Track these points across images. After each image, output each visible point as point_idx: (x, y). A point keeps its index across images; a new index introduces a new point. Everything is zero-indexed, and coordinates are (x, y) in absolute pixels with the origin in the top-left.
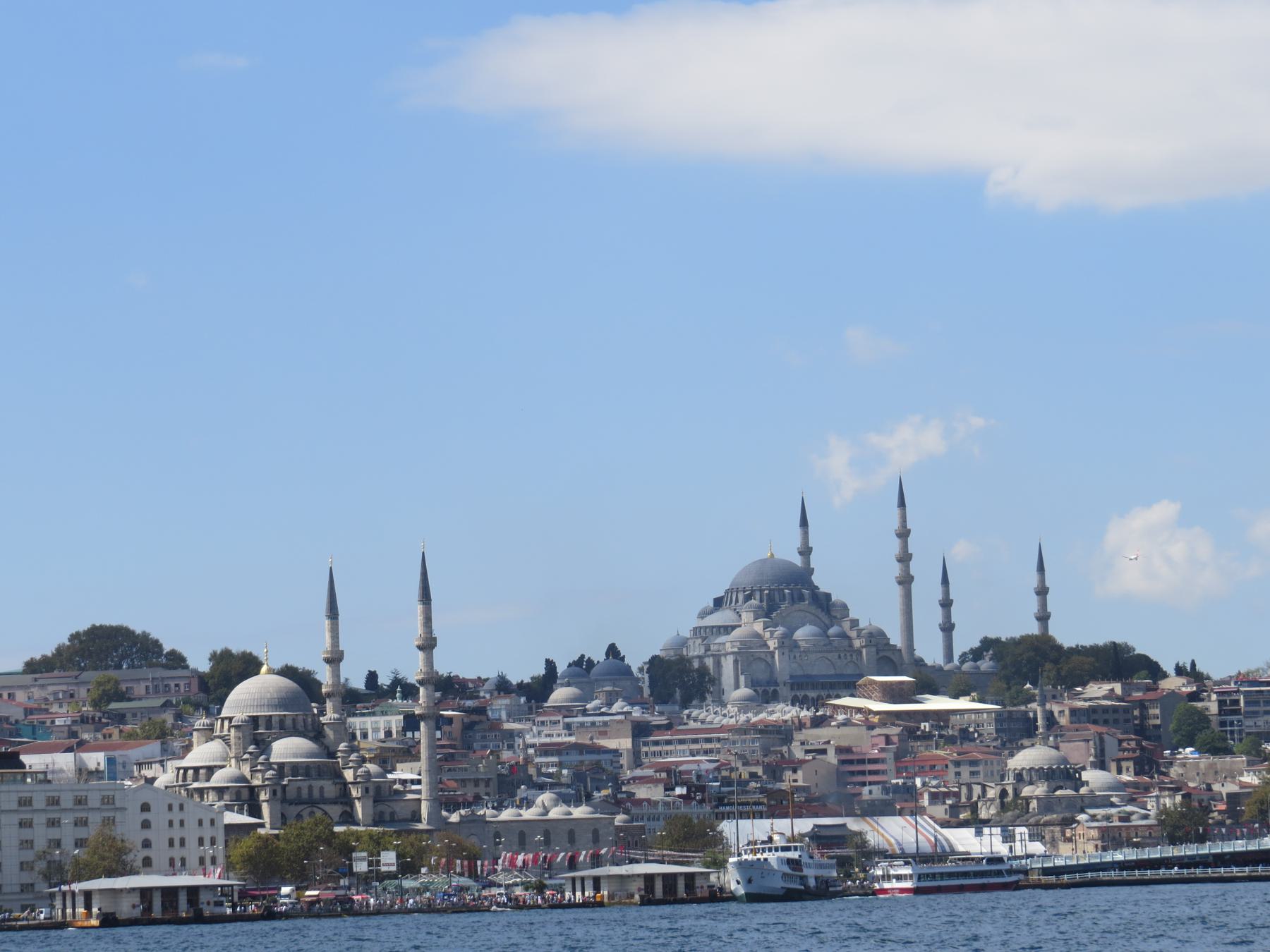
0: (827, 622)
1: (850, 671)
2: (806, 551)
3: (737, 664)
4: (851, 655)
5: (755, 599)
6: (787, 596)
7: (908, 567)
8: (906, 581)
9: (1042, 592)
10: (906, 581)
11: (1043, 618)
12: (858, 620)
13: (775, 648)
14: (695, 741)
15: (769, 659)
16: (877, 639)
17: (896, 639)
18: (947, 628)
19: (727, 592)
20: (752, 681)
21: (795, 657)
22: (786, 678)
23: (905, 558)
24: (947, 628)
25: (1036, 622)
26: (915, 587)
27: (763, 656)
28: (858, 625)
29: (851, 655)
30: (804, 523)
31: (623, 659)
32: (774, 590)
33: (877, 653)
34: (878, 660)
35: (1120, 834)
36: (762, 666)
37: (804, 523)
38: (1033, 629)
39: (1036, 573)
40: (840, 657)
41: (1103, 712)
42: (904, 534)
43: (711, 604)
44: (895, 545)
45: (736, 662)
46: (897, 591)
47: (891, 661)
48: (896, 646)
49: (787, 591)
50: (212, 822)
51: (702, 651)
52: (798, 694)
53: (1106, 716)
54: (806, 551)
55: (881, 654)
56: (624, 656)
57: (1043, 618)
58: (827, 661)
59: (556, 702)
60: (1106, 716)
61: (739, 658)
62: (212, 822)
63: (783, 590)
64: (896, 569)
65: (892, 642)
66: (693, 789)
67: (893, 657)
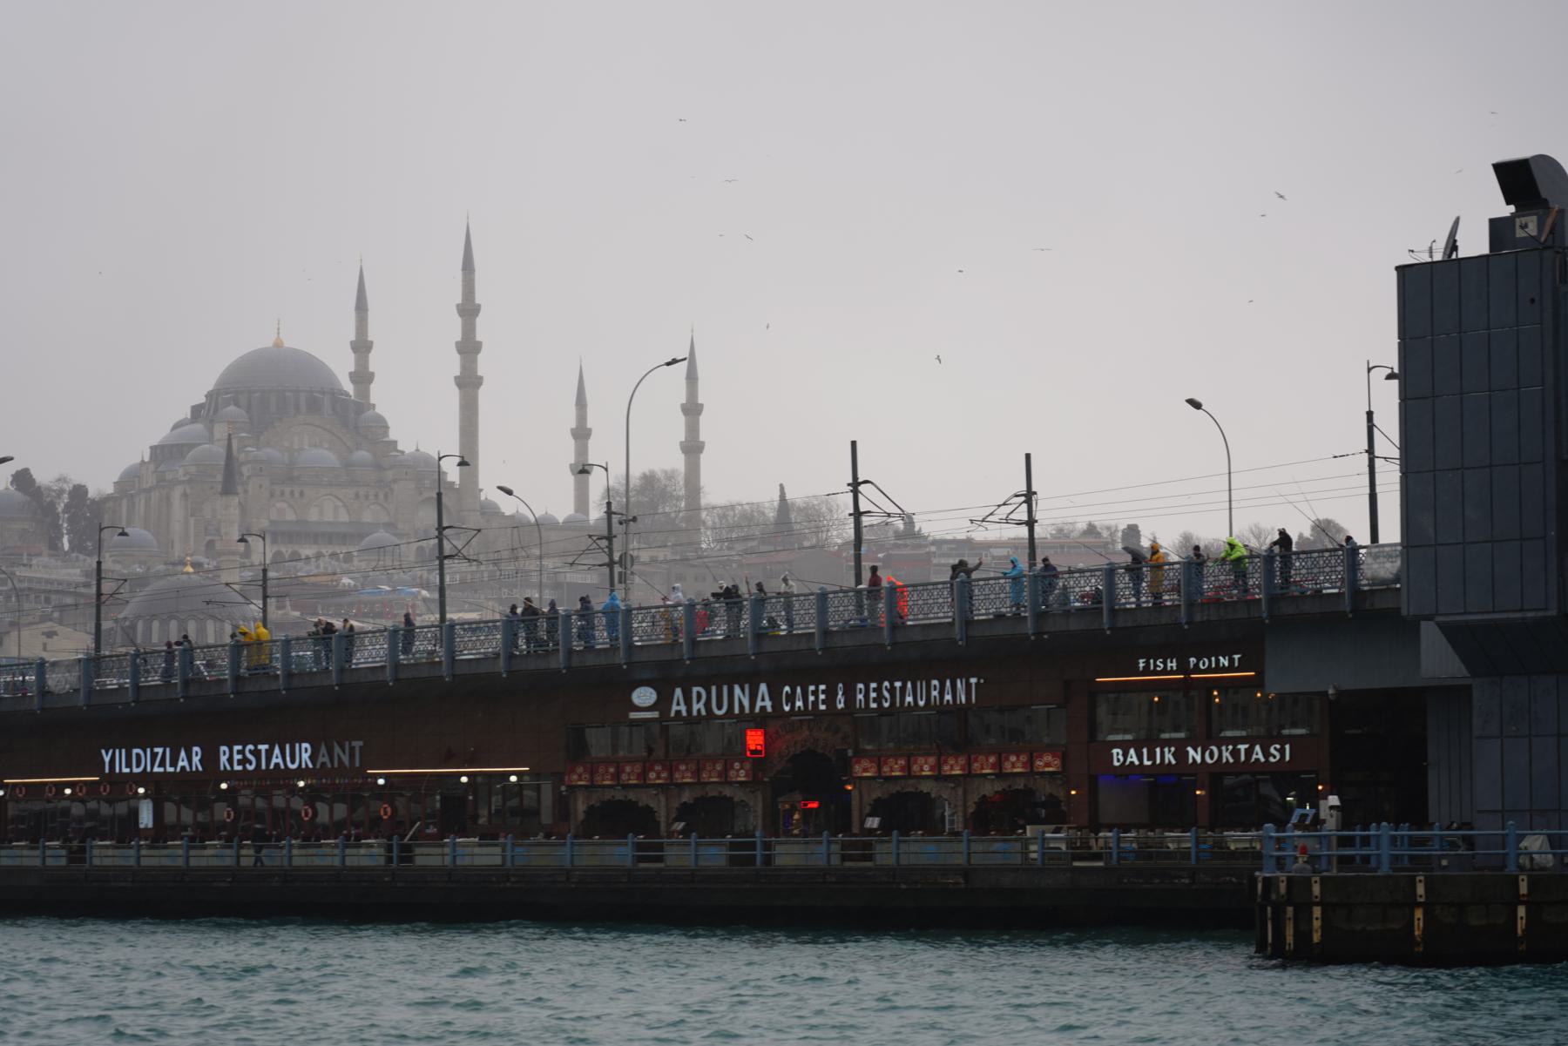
2: (362, 347)
4: (376, 496)
5: (237, 404)
7: (474, 361)
8: (469, 383)
10: (469, 383)
11: (692, 448)
13: (249, 477)
16: (426, 471)
19: (209, 395)
20: (206, 529)
21: (282, 493)
23: (469, 348)
25: (683, 456)
26: (483, 394)
29: (376, 496)
39: (685, 381)
40: (357, 496)
41: (696, 579)
43: (189, 417)
44: (454, 328)
45: (185, 495)
46: (454, 395)
51: (155, 484)
52: (284, 550)
54: (362, 347)
57: (692, 448)
61: (188, 491)
64: (454, 365)
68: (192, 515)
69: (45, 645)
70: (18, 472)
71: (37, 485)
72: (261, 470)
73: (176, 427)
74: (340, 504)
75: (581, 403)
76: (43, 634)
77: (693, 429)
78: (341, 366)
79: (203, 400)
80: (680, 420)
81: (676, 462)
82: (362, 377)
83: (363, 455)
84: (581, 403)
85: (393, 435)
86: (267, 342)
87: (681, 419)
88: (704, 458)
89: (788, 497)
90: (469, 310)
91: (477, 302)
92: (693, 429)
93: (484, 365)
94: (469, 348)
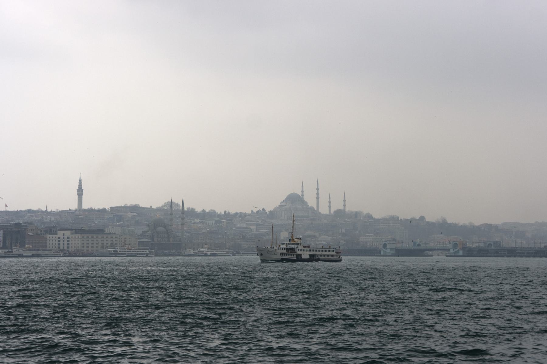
2: (302, 192)
8: (318, 198)
10: (318, 198)
11: (345, 206)
14: (267, 227)
17: (316, 209)
18: (330, 207)
23: (318, 194)
24: (330, 207)
31: (265, 211)
50: (136, 241)
54: (302, 192)
57: (345, 206)
62: (136, 241)
73: (281, 203)
75: (330, 198)
77: (345, 203)
78: (300, 194)
82: (303, 195)
83: (305, 207)
84: (330, 198)
85: (308, 204)
86: (292, 192)
87: (343, 202)
88: (346, 207)
92: (345, 203)
93: (320, 196)
94: (318, 194)
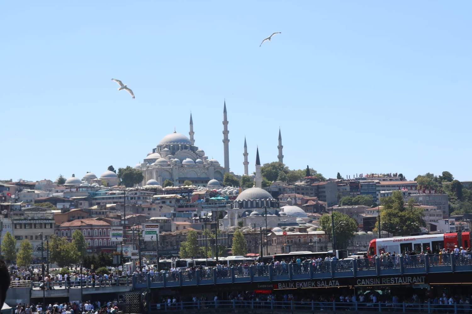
0: (196, 158)
1: (203, 176)
2: (192, 133)
3: (157, 173)
6: (180, 147)
7: (227, 136)
8: (226, 141)
9: (280, 147)
10: (226, 141)
11: (281, 157)
12: (207, 157)
15: (170, 171)
16: (214, 164)
17: (222, 165)
22: (177, 178)
23: (226, 132)
27: (168, 170)
28: (207, 159)
30: (191, 123)
32: (175, 145)
33: (215, 169)
34: (215, 172)
35: (300, 240)
36: (168, 173)
37: (191, 123)
38: (277, 160)
41: (302, 190)
42: (226, 123)
47: (220, 172)
48: (222, 167)
49: (180, 145)
53: (303, 191)
54: (192, 133)
55: (216, 170)
56: (115, 171)
57: (281, 157)
58: (194, 172)
59: (68, 183)
60: (303, 191)
61: (158, 170)
63: (178, 145)
65: (221, 166)
66: (3, 208)
67: (221, 171)
68: (159, 176)
69: (160, 210)
70: (109, 167)
71: (115, 170)
72: (176, 164)
74: (195, 173)
75: (245, 146)
76: (160, 207)
77: (281, 152)
78: (188, 137)
79: (156, 147)
80: (277, 151)
81: (277, 160)
82: (193, 140)
84: (245, 146)
87: (278, 150)
89: (309, 168)
90: (226, 123)
91: (228, 120)
93: (230, 137)
94: (226, 132)
